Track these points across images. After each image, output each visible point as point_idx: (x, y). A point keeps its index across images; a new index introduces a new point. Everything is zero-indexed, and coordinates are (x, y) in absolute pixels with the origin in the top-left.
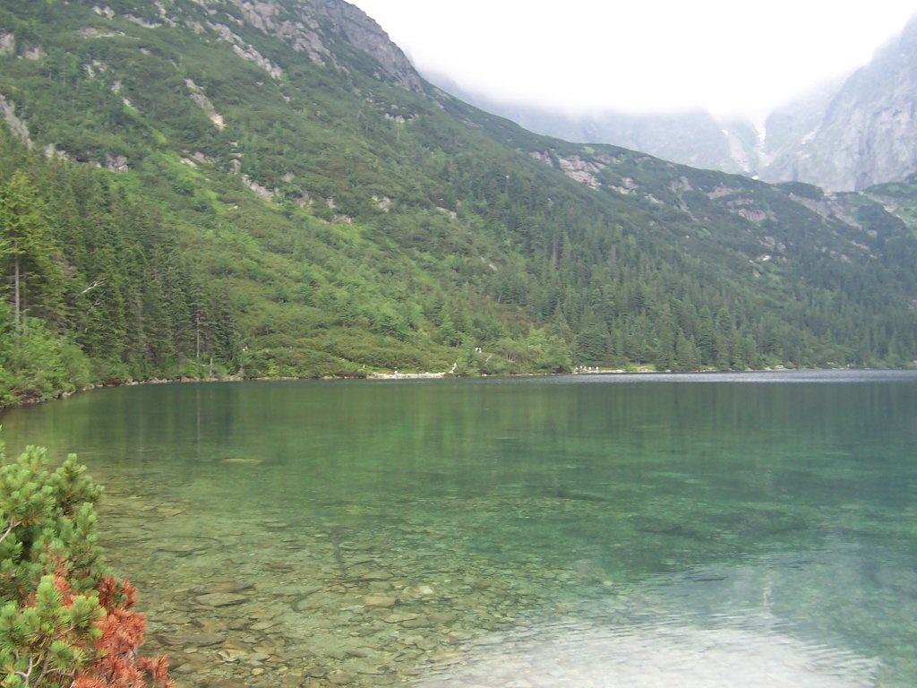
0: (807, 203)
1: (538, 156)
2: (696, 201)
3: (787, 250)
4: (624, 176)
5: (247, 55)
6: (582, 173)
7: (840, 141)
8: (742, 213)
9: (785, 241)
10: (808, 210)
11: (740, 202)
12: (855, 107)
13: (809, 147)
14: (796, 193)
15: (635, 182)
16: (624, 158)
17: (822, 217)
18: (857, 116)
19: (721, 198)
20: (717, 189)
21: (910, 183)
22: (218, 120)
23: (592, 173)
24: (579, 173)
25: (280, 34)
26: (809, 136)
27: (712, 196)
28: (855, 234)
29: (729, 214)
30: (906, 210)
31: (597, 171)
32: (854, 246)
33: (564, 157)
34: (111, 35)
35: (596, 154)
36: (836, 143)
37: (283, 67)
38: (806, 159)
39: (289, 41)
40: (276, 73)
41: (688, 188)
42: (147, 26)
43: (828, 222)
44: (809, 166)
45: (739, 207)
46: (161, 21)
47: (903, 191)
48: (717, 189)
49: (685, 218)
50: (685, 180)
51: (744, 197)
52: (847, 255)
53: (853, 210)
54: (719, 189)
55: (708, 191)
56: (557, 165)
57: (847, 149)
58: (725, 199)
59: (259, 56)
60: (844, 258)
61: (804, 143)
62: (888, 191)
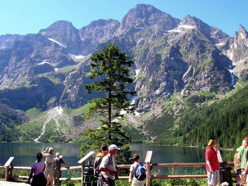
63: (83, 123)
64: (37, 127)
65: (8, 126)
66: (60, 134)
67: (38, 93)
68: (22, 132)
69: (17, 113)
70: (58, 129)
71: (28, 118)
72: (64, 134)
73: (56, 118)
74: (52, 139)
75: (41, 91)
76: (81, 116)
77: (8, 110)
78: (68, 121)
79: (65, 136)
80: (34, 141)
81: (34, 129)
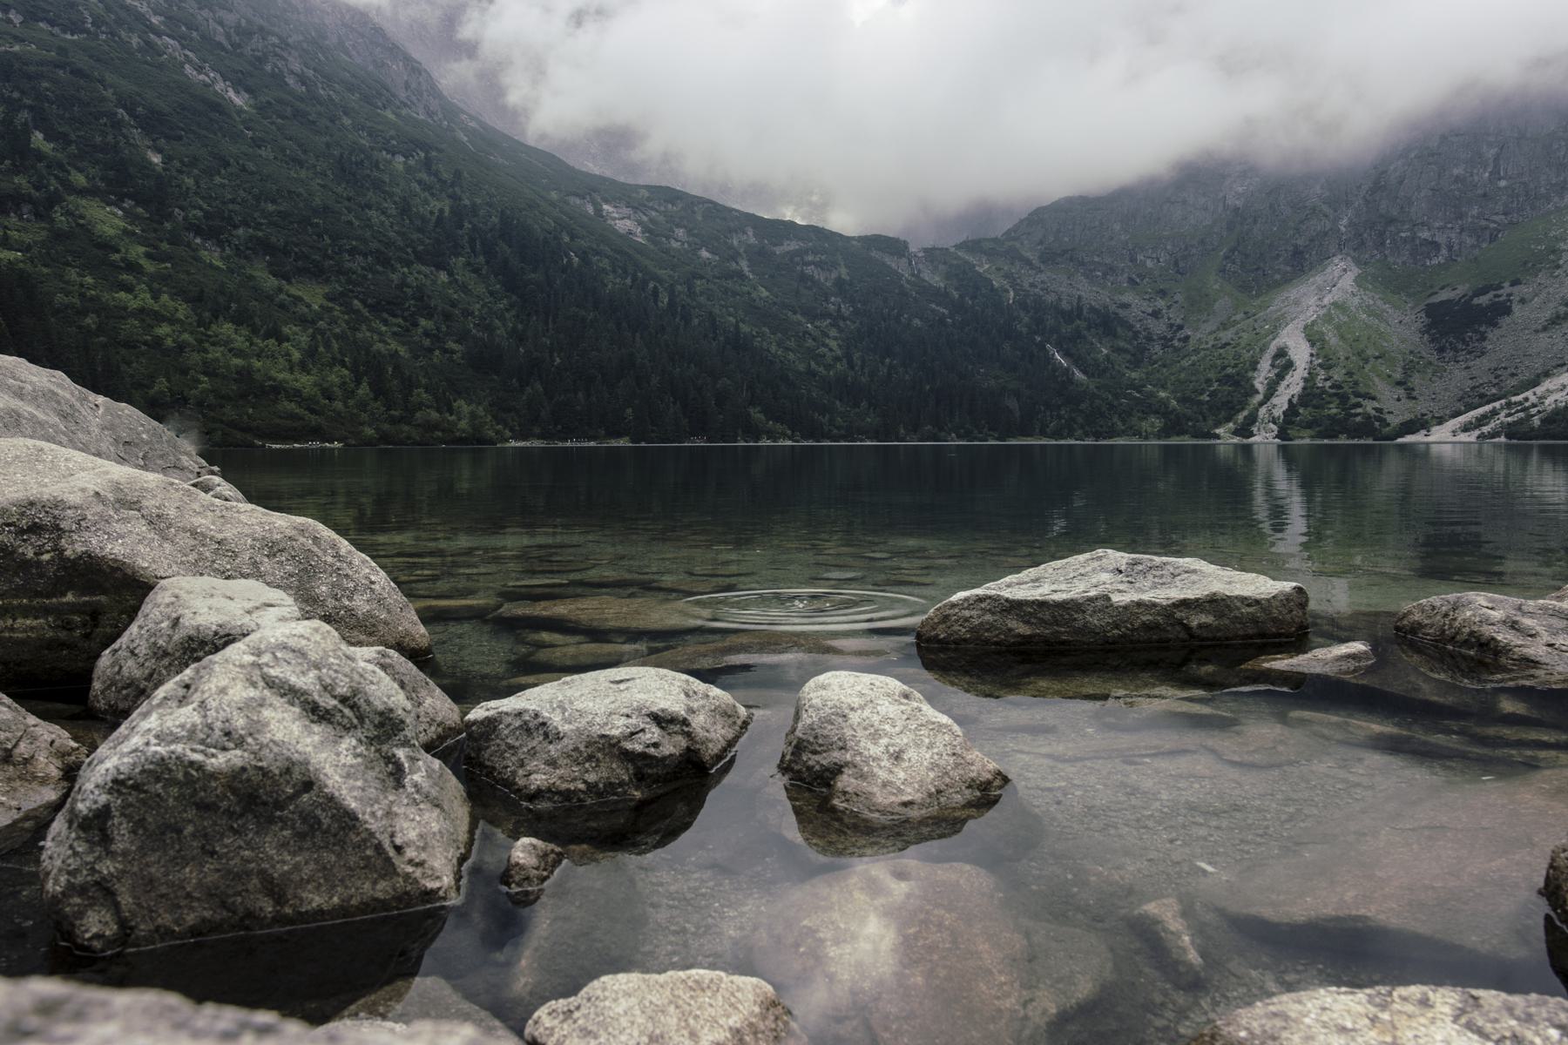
0: (890, 261)
1: (578, 201)
2: (759, 256)
4: (678, 226)
5: (202, 77)
6: (628, 222)
8: (809, 270)
11: (810, 258)
15: (689, 232)
16: (680, 205)
22: (156, 159)
23: (640, 223)
24: (623, 223)
25: (247, 51)
27: (778, 250)
30: (999, 269)
31: (645, 218)
32: (933, 311)
33: (607, 202)
34: (17, 48)
35: (649, 199)
37: (249, 90)
39: (259, 59)
40: (238, 100)
41: (753, 240)
42: (68, 37)
43: (908, 282)
45: (809, 264)
46: (88, 32)
49: (741, 275)
50: (750, 233)
51: (815, 253)
53: (941, 267)
56: (598, 211)
59: (218, 77)
60: (917, 322)
63: (1490, 335)
64: (1230, 370)
65: (1085, 372)
66: (1354, 400)
67: (1229, 202)
68: (1152, 395)
69: (1126, 306)
70: (1338, 375)
71: (1180, 327)
72: (1374, 399)
73: (1328, 318)
74: (1309, 425)
75: (1240, 189)
76: (1476, 301)
77: (1080, 297)
78: (1401, 327)
79: (1379, 410)
80: (1217, 437)
81: (1212, 375)
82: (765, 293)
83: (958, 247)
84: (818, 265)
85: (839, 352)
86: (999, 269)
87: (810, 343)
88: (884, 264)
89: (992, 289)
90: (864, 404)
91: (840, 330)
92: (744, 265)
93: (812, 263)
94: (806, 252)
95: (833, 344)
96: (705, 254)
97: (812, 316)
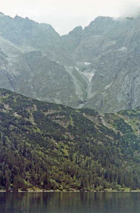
0: (90, 118)
3: (75, 139)
7: (120, 89)
8: (57, 122)
9: (75, 135)
10: (90, 121)
11: (57, 117)
12: (126, 74)
13: (107, 91)
14: (87, 113)
17: (95, 124)
18: (127, 78)
19: (50, 115)
20: (49, 110)
21: (137, 110)
26: (108, 86)
28: (110, 132)
29: (52, 122)
32: (107, 138)
36: (118, 90)
38: (106, 96)
41: (36, 110)
43: (98, 126)
44: (107, 99)
47: (133, 113)
48: (49, 110)
49: (29, 123)
50: (35, 106)
51: (61, 114)
52: (102, 141)
54: (50, 110)
55: (45, 111)
57: (123, 92)
58: (52, 115)
61: (106, 89)
62: (127, 113)
82: (39, 130)
83: (118, 113)
84: (61, 119)
85: (67, 154)
86: (134, 122)
87: (55, 150)
88: (88, 119)
89: (132, 131)
90: (75, 177)
91: (69, 146)
92: (32, 120)
93: (59, 119)
94: (57, 114)
95: (66, 151)
96: (16, 115)
97: (58, 140)
